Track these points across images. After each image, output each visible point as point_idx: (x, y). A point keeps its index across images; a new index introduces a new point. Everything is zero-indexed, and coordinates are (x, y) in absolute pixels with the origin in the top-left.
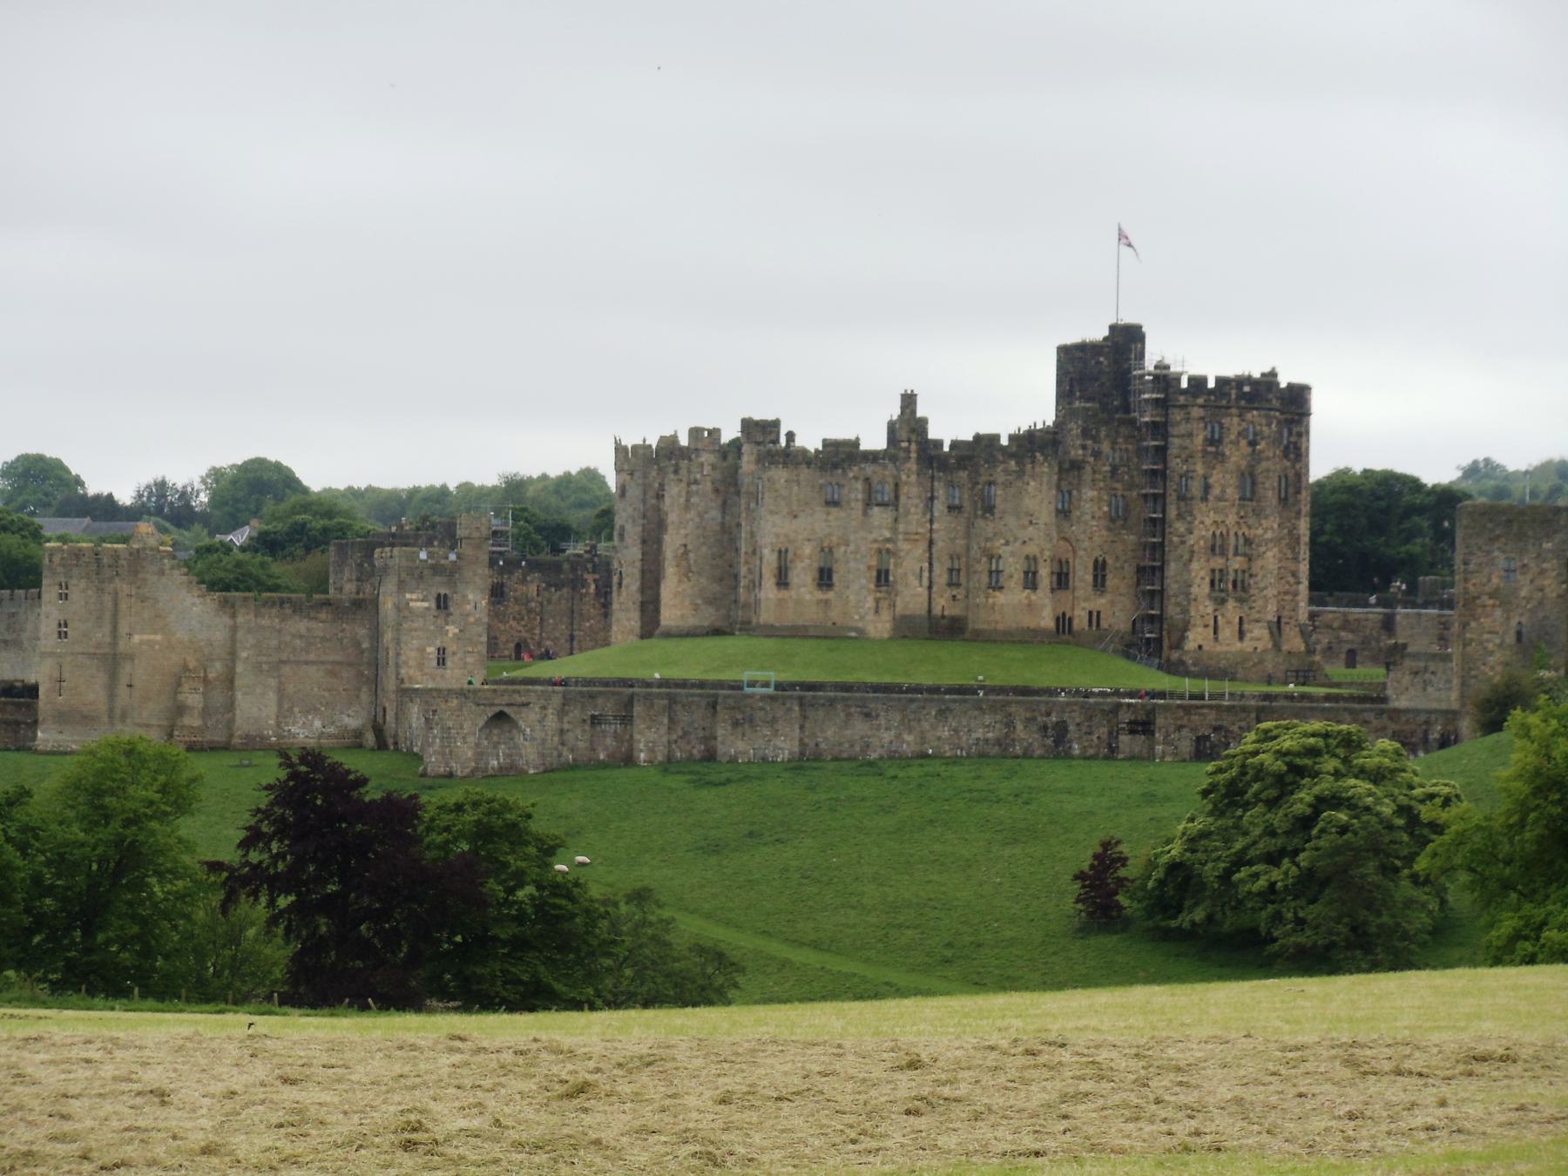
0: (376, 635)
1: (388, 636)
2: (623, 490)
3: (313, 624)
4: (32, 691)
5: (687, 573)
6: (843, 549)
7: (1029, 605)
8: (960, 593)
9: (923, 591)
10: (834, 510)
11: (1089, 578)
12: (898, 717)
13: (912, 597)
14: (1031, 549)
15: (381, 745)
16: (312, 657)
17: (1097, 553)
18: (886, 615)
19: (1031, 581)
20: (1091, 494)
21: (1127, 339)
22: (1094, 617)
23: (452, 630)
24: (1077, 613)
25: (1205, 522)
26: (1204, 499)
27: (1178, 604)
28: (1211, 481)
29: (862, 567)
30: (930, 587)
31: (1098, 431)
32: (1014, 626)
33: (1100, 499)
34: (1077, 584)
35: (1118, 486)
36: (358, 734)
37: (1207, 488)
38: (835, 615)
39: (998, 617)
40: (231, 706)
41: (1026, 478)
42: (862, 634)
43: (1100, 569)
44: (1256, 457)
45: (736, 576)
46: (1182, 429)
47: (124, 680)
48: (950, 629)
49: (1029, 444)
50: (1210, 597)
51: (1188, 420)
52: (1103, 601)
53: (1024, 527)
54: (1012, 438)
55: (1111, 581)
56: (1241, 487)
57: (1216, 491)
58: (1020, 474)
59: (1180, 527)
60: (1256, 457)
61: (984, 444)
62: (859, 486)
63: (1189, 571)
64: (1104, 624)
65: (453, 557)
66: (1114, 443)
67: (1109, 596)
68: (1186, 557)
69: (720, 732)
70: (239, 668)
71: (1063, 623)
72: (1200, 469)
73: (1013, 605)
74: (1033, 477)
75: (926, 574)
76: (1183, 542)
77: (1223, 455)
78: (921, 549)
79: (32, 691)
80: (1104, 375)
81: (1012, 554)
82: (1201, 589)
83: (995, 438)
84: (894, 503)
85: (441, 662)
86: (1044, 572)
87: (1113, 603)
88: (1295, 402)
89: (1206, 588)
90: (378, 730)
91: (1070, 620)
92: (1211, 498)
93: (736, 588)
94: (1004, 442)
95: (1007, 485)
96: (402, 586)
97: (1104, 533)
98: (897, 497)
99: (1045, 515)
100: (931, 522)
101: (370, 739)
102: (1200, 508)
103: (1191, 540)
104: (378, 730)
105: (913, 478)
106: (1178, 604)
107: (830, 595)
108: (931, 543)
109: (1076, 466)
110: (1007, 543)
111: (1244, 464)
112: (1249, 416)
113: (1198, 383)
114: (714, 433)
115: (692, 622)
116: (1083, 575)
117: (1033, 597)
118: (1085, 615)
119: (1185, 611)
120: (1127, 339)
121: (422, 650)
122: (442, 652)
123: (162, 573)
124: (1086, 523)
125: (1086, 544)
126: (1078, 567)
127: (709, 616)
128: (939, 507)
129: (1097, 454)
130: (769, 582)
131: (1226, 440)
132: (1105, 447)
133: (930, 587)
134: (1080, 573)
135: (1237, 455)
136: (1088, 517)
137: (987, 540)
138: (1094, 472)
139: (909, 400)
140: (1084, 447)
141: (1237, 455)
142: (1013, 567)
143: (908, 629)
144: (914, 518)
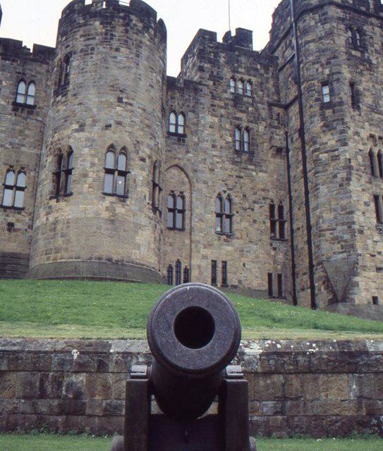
14: (121, 137)
17: (220, 188)
20: (210, 119)
24: (195, 262)
27: (337, 239)
28: (361, 88)
31: (216, 55)
32: (84, 255)
34: (196, 224)
39: (60, 241)
41: (115, 43)
46: (320, 30)
51: (324, 22)
52: (229, 248)
53: (110, 105)
55: (240, 224)
58: (108, 37)
59: (330, 140)
63: (348, 194)
66: (235, 71)
67: (237, 243)
68: (343, 174)
72: (346, 74)
76: (335, 158)
77: (370, 63)
81: (91, 142)
86: (140, 175)
92: (363, 107)
95: (88, 51)
97: (228, 165)
102: (349, 112)
103: (347, 153)
106: (337, 239)
110: (82, 128)
116: (203, 215)
117: (120, 209)
118: (207, 265)
119: (349, 247)
125: (208, 175)
126: (196, 203)
129: (216, 79)
131: (370, 49)
132: (226, 72)
134: (198, 210)
136: (207, 145)
137: (55, 130)
138: (214, 97)
140: (201, 69)
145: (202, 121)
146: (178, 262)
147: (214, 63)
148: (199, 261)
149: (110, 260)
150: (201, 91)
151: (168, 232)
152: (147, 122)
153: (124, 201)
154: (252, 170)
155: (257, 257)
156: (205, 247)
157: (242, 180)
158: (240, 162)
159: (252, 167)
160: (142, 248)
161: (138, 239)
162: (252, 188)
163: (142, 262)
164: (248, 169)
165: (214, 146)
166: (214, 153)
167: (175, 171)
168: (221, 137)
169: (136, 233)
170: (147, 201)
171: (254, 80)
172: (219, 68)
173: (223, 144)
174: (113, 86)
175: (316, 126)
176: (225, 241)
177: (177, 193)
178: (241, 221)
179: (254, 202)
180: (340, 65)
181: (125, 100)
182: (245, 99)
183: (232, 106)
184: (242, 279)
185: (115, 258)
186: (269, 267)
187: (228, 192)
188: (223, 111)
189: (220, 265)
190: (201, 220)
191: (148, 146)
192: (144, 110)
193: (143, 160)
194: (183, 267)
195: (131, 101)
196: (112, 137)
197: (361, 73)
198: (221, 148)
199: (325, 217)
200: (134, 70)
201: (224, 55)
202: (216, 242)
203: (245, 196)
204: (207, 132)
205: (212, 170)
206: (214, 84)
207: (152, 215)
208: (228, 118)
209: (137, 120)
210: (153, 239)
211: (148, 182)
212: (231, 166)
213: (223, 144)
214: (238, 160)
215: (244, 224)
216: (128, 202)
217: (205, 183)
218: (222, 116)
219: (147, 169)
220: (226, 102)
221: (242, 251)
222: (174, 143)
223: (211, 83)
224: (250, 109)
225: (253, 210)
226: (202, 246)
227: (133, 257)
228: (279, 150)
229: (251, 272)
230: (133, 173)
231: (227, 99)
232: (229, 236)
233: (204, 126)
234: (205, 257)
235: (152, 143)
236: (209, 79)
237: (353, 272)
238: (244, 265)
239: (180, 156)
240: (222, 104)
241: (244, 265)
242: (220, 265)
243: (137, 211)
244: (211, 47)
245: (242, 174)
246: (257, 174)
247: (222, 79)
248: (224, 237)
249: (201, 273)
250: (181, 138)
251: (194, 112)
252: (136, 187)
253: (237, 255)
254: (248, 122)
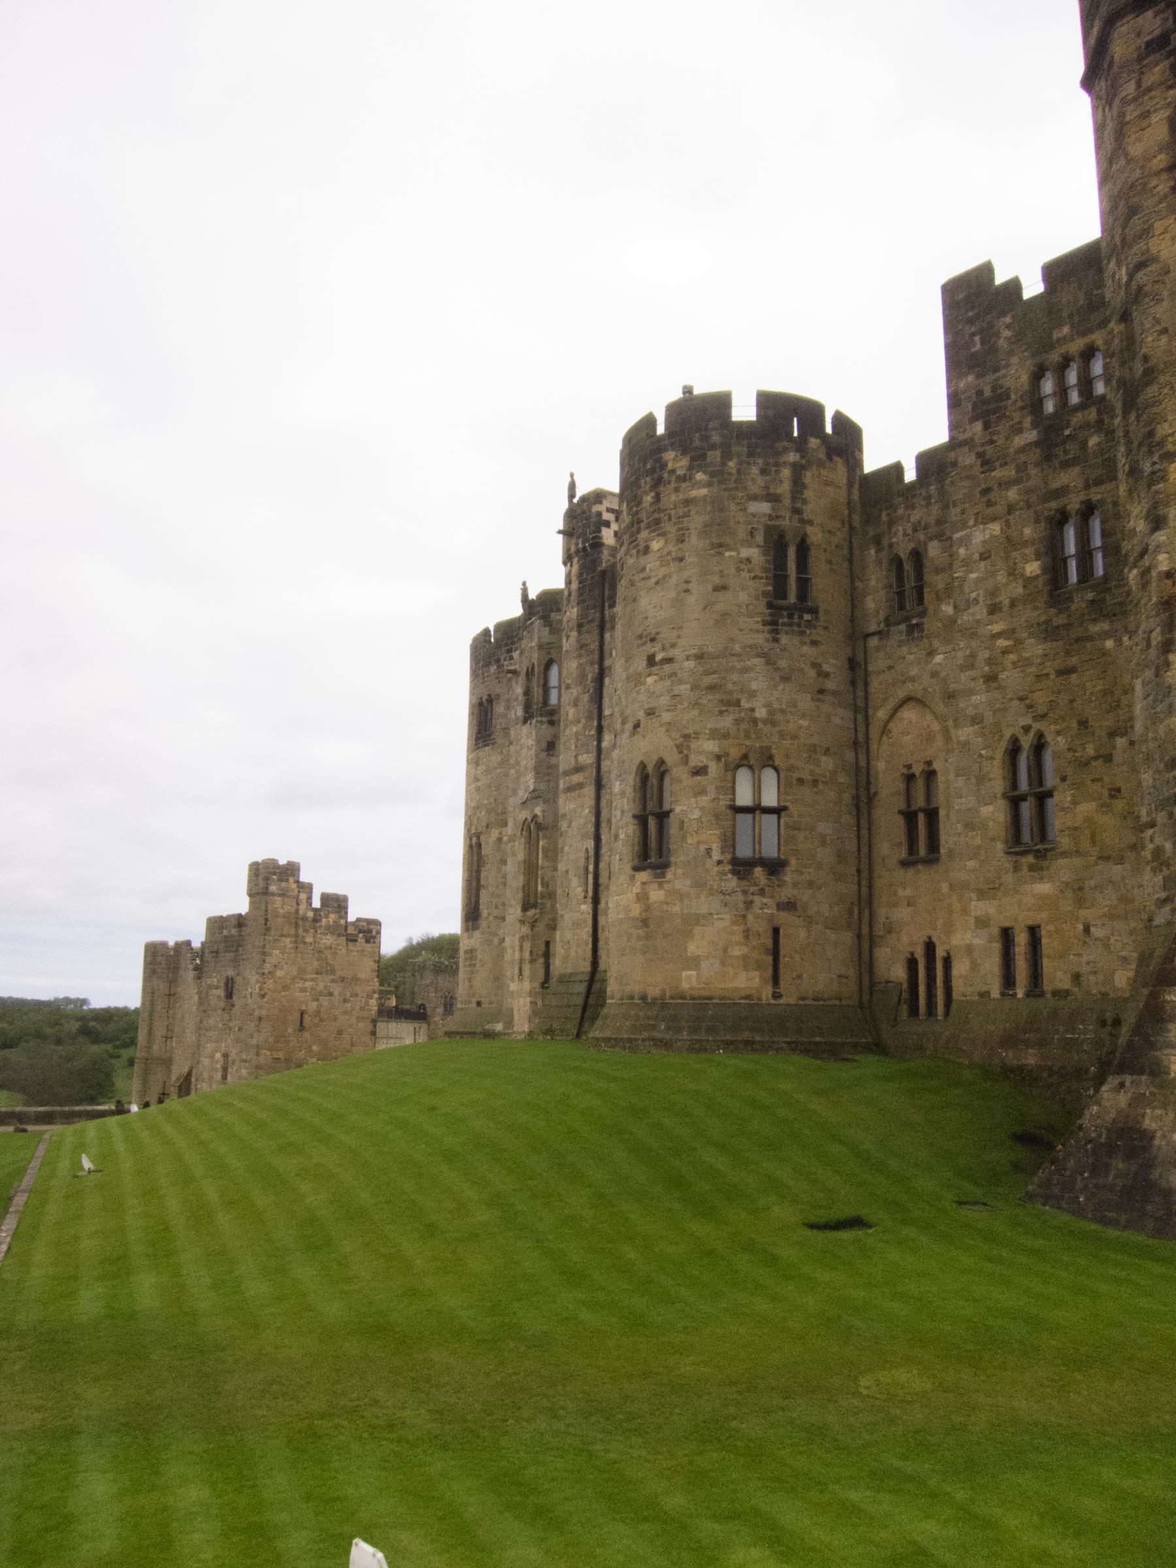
6: (495, 833)
7: (645, 922)
11: (995, 813)
17: (1016, 722)
33: (1011, 543)
35: (1070, 478)
52: (1045, 888)
64: (1056, 975)
67: (1064, 869)
87: (1079, 892)
91: (947, 961)
97: (1034, 648)
108: (599, 785)
117: (656, 895)
124: (971, 633)
138: (987, 463)
145: (962, 551)
146: (930, 947)
148: (969, 935)
149: (644, 997)
150: (954, 464)
151: (901, 872)
152: (708, 680)
153: (663, 875)
154: (1107, 635)
155: (1123, 900)
156: (982, 894)
157: (1074, 676)
158: (1069, 626)
159: (1105, 626)
160: (703, 965)
161: (692, 948)
162: (1106, 692)
163: (707, 994)
164: (1089, 638)
165: (994, 609)
166: (997, 628)
167: (909, 714)
168: (1012, 573)
169: (688, 934)
170: (716, 855)
171: (1098, 338)
172: (996, 369)
173: (1018, 590)
174: (640, 637)
176: (1032, 868)
177: (917, 770)
178: (1074, 803)
179: (1112, 735)
180: (1146, 232)
181: (658, 657)
182: (1077, 418)
183: (1037, 464)
184: (1085, 969)
185: (653, 992)
187: (1037, 726)
188: (1012, 494)
189: (1021, 939)
190: (970, 826)
191: (715, 734)
192: (699, 657)
193: (700, 771)
194: (940, 953)
195: (671, 653)
198: (1013, 604)
200: (675, 578)
201: (1008, 320)
202: (1009, 878)
203: (1083, 723)
204: (973, 576)
205: (991, 678)
206: (986, 426)
207: (732, 882)
208: (1029, 507)
209: (684, 689)
210: (738, 937)
211: (717, 816)
212: (1039, 650)
213: (1018, 590)
214: (1060, 620)
215: (1087, 808)
216: (669, 875)
217: (976, 720)
218: (1011, 509)
219: (711, 789)
220: (1023, 458)
221: (1081, 889)
222: (901, 644)
223: (978, 426)
224: (1093, 441)
225: (1108, 759)
226: (973, 895)
227: (685, 985)
229: (1107, 946)
230: (678, 809)
231: (1023, 450)
232: (1041, 855)
233: (967, 564)
234: (982, 923)
235: (726, 722)
236: (973, 420)
238: (1087, 930)
239: (914, 672)
240: (1009, 472)
241: (1087, 930)
242: (1021, 939)
244: (970, 321)
245: (1074, 660)
246: (1119, 641)
247: (1008, 397)
248: (1030, 859)
249: (974, 966)
251: (939, 536)
252: (684, 838)
253: (1067, 906)
254: (1087, 486)
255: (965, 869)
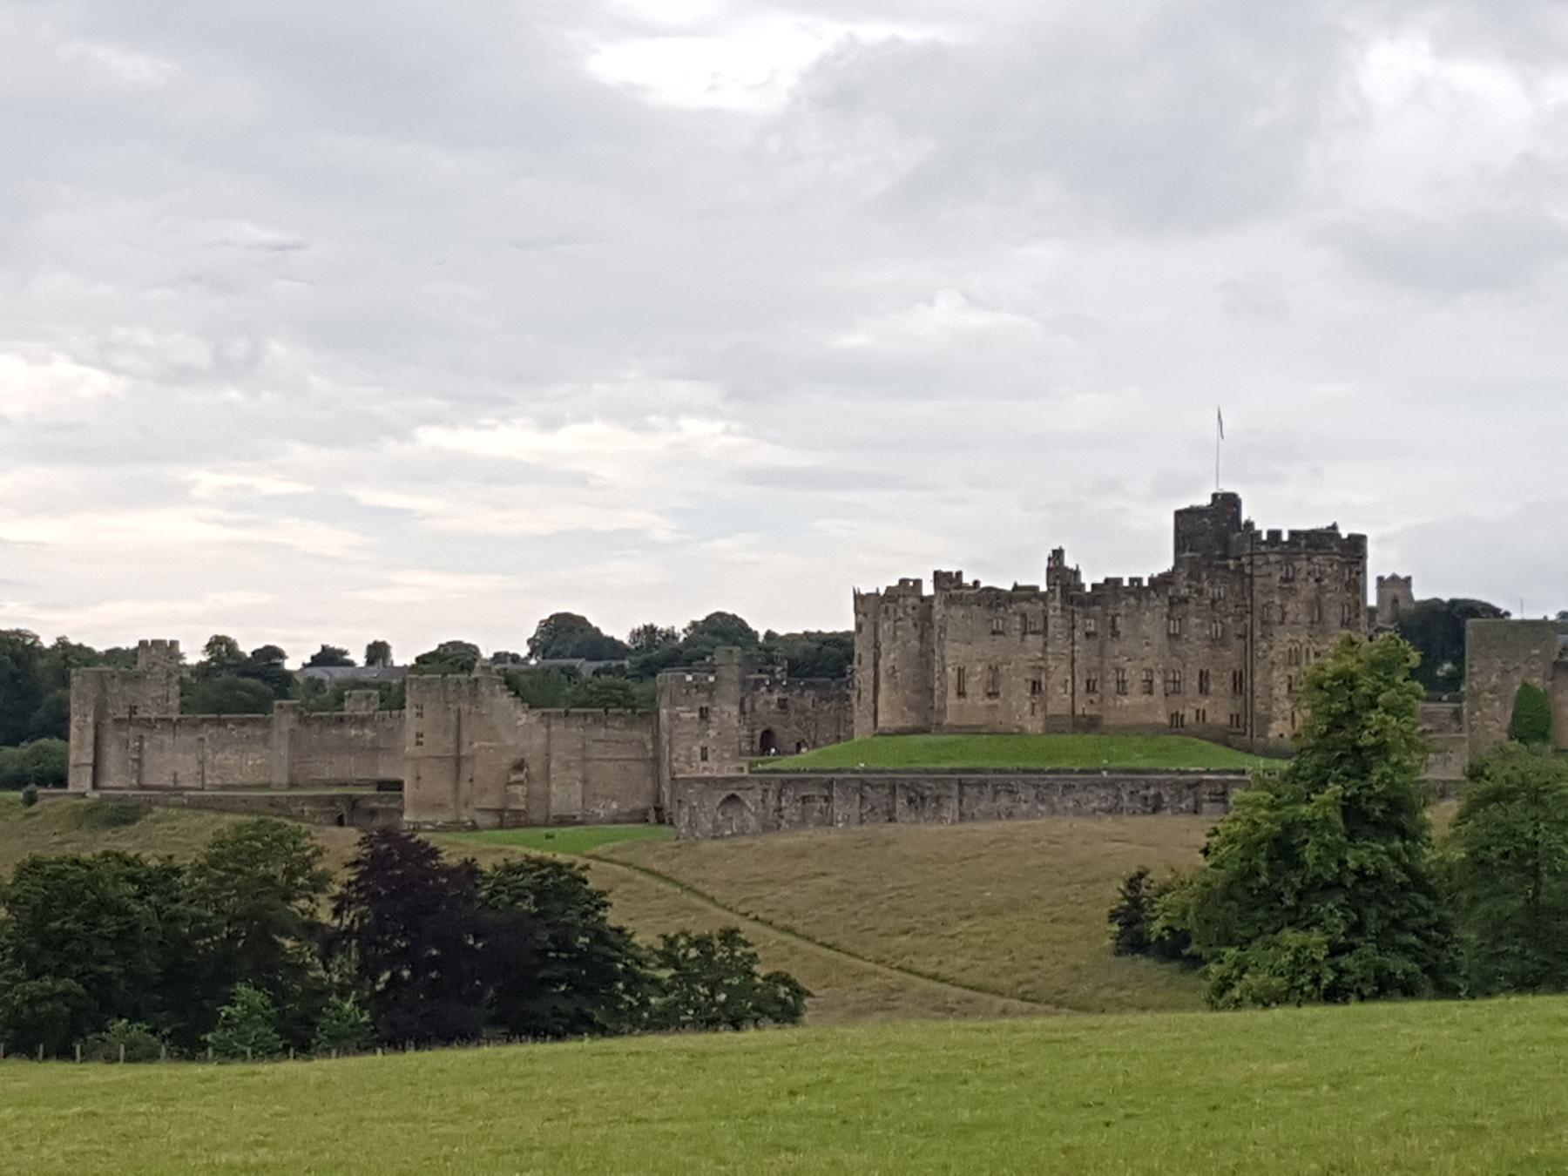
0: (656, 739)
1: (665, 737)
2: (859, 626)
3: (611, 731)
4: (398, 785)
5: (895, 687)
8: (1095, 698)
9: (1068, 696)
10: (997, 637)
11: (1196, 684)
12: (1033, 792)
13: (1059, 702)
14: (1148, 664)
15: (661, 822)
16: (609, 756)
18: (1039, 715)
19: (1149, 689)
21: (1227, 504)
22: (1201, 715)
23: (712, 733)
25: (1283, 640)
26: (1282, 623)
29: (1021, 680)
30: (1073, 694)
36: (645, 812)
37: (1284, 614)
38: (1000, 716)
40: (547, 795)
42: (1022, 732)
43: (1204, 677)
44: (1321, 590)
45: (932, 690)
46: (1265, 570)
47: (465, 776)
48: (1091, 724)
49: (1160, 582)
50: (1288, 697)
51: (1268, 563)
54: (1151, 580)
56: (1311, 614)
57: (1290, 617)
59: (1265, 645)
60: (1321, 590)
61: (1112, 583)
62: (1018, 619)
64: (1208, 720)
65: (712, 679)
69: (898, 806)
70: (553, 765)
71: (1176, 720)
72: (1277, 601)
73: (1133, 705)
74: (1148, 609)
75: (1069, 685)
78: (1065, 666)
79: (398, 785)
80: (1211, 532)
82: (1281, 691)
83: (1119, 581)
84: (1044, 632)
85: (704, 758)
88: (1357, 545)
89: (1285, 691)
90: (658, 810)
93: (932, 698)
94: (1126, 583)
96: (673, 703)
98: (1046, 627)
99: (1159, 638)
100: (1073, 644)
101: (652, 816)
103: (1272, 654)
104: (658, 810)
105: (1058, 612)
107: (995, 701)
109: (1185, 601)
111: (1312, 595)
112: (1315, 560)
113: (1275, 535)
114: (918, 583)
115: (900, 724)
119: (1269, 708)
120: (1227, 504)
121: (689, 749)
122: (704, 750)
123: (493, 694)
127: (911, 720)
128: (1078, 634)
129: (1200, 592)
130: (952, 693)
133: (1073, 694)
135: (1307, 589)
139: (1058, 554)
140: (1189, 586)
141: (1307, 589)
142: (1134, 676)
143: (1053, 725)
144: (1060, 644)
147: (1199, 580)
175: (1258, 633)
186: (1233, 711)
196: (1146, 664)
197: (1287, 599)
199: (1259, 690)
228: (1240, 636)
237: (1269, 720)
243: (1158, 696)
250: (1176, 637)
255: (1189, 696)
